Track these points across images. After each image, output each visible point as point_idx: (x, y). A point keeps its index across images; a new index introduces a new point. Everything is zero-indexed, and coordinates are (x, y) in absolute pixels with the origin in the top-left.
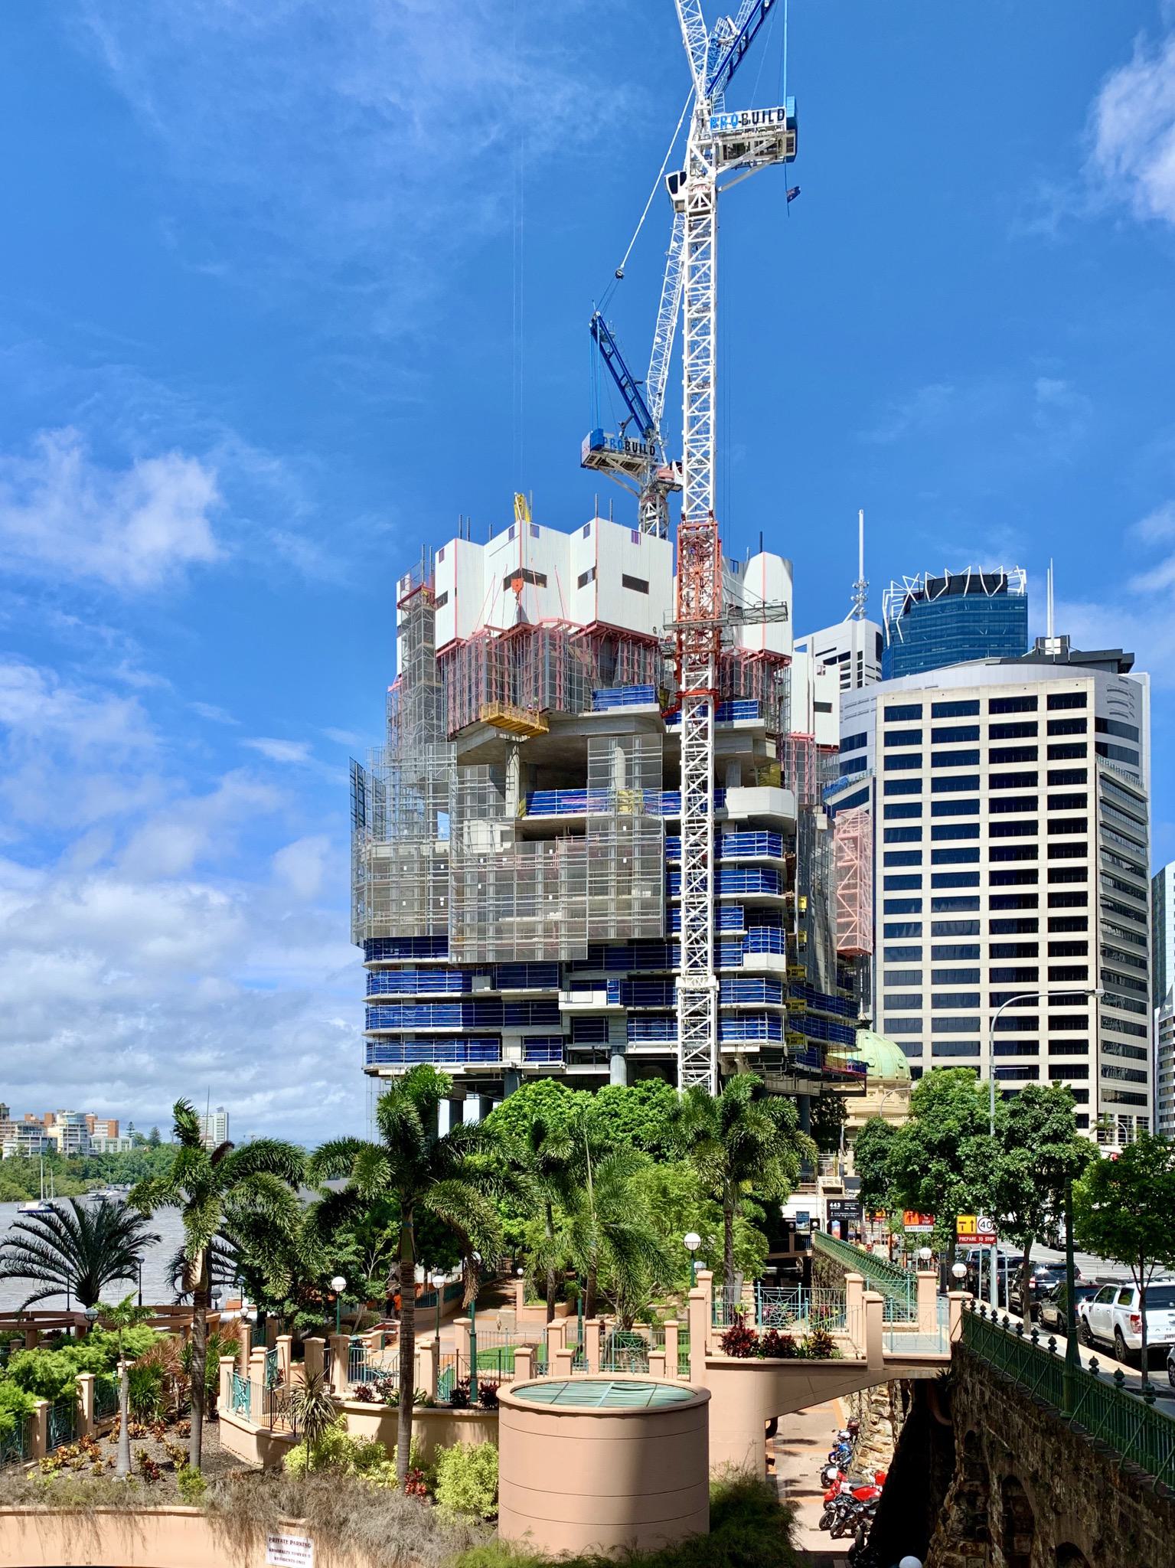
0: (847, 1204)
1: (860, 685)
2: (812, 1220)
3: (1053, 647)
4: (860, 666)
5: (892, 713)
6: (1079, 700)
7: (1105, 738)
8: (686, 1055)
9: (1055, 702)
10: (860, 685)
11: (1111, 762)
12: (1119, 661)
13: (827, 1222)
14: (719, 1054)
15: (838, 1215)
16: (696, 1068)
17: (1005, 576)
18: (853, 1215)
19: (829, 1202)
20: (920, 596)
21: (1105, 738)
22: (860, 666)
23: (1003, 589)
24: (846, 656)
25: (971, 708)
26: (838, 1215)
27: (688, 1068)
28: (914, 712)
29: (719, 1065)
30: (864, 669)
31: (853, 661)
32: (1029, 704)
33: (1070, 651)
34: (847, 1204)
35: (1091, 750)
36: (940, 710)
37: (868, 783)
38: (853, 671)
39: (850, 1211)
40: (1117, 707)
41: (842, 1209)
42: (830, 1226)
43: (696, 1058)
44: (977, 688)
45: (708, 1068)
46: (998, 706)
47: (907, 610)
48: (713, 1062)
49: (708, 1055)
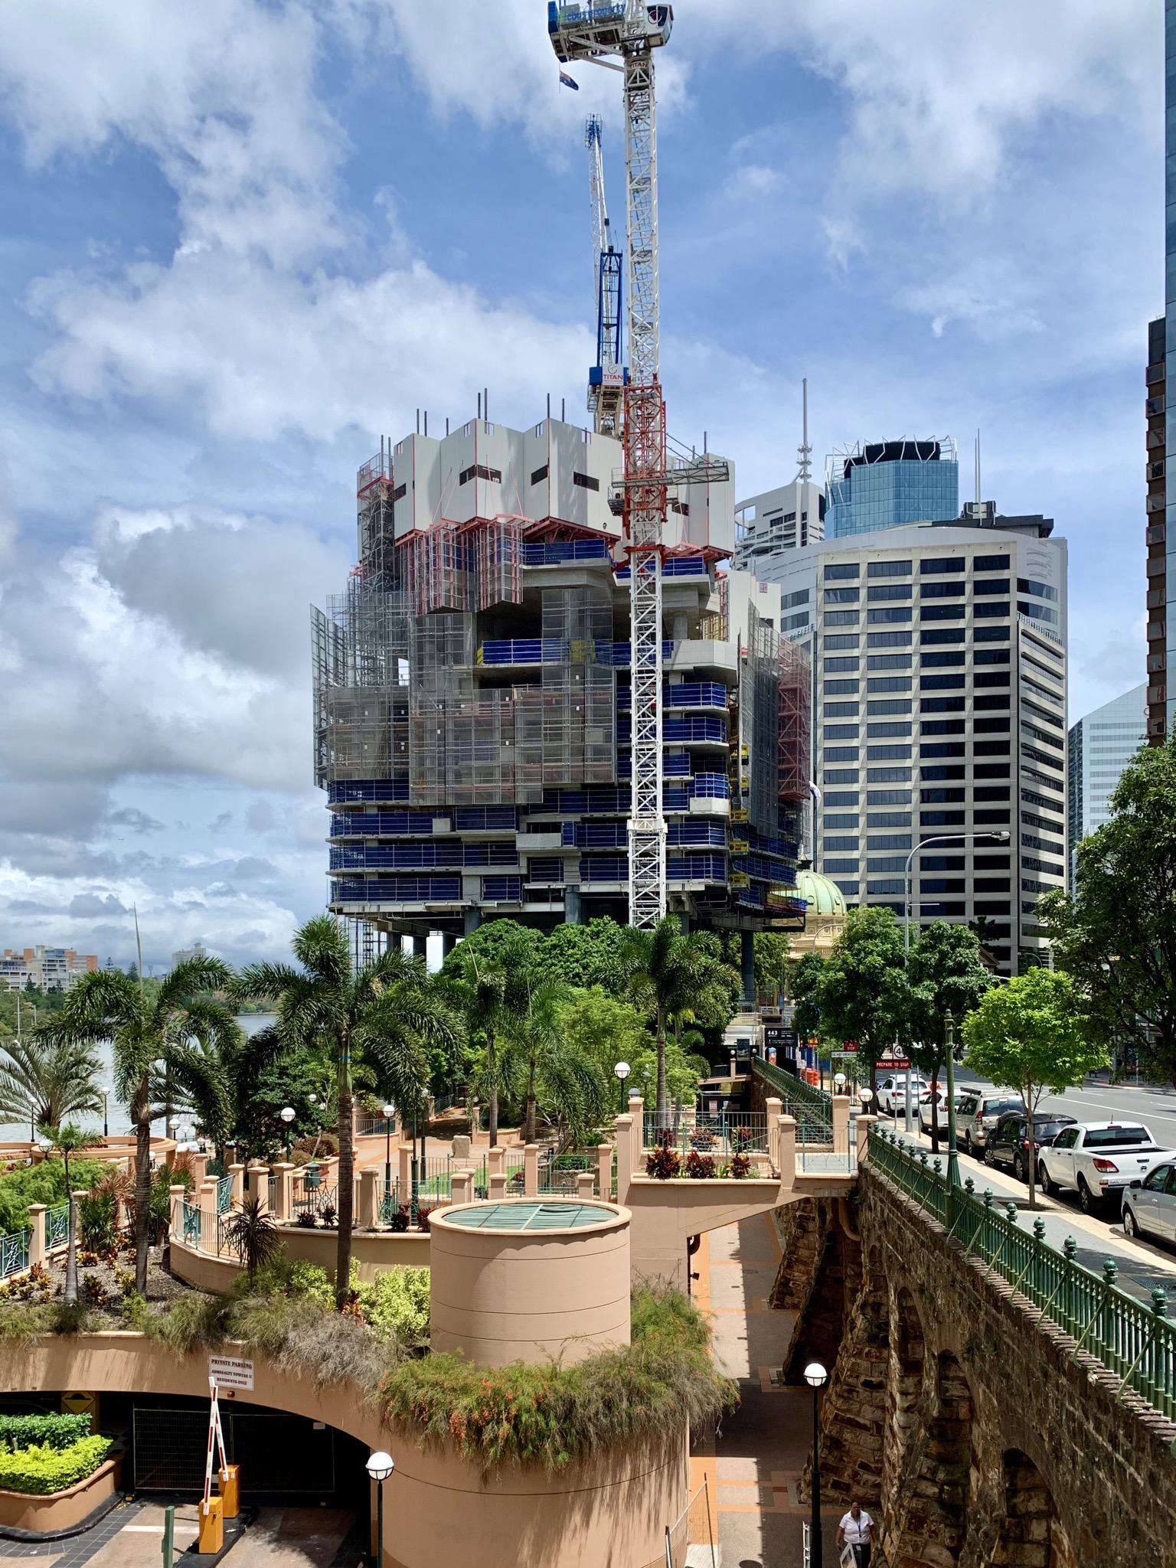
0: (784, 1032)
1: (804, 544)
2: (753, 1047)
3: (980, 514)
4: (804, 526)
5: (832, 572)
6: (1003, 562)
7: (1025, 598)
8: (637, 894)
9: (981, 563)
10: (804, 544)
11: (1032, 620)
12: (1039, 526)
13: (764, 1049)
14: (668, 893)
15: (776, 1042)
16: (646, 906)
17: (937, 445)
18: (790, 1042)
19: (767, 1030)
20: (859, 461)
21: (1025, 598)
22: (804, 526)
23: (936, 456)
24: (792, 516)
25: (903, 567)
26: (776, 1042)
27: (638, 906)
28: (851, 571)
29: (667, 903)
30: (810, 531)
31: (798, 521)
32: (956, 565)
33: (996, 515)
34: (784, 1032)
35: (1013, 608)
36: (875, 569)
37: (810, 637)
38: (798, 530)
39: (786, 1038)
40: (1037, 569)
41: (779, 1037)
42: (767, 1053)
43: (646, 896)
44: (910, 549)
45: (657, 906)
46: (927, 566)
47: (848, 474)
48: (663, 900)
49: (658, 894)
